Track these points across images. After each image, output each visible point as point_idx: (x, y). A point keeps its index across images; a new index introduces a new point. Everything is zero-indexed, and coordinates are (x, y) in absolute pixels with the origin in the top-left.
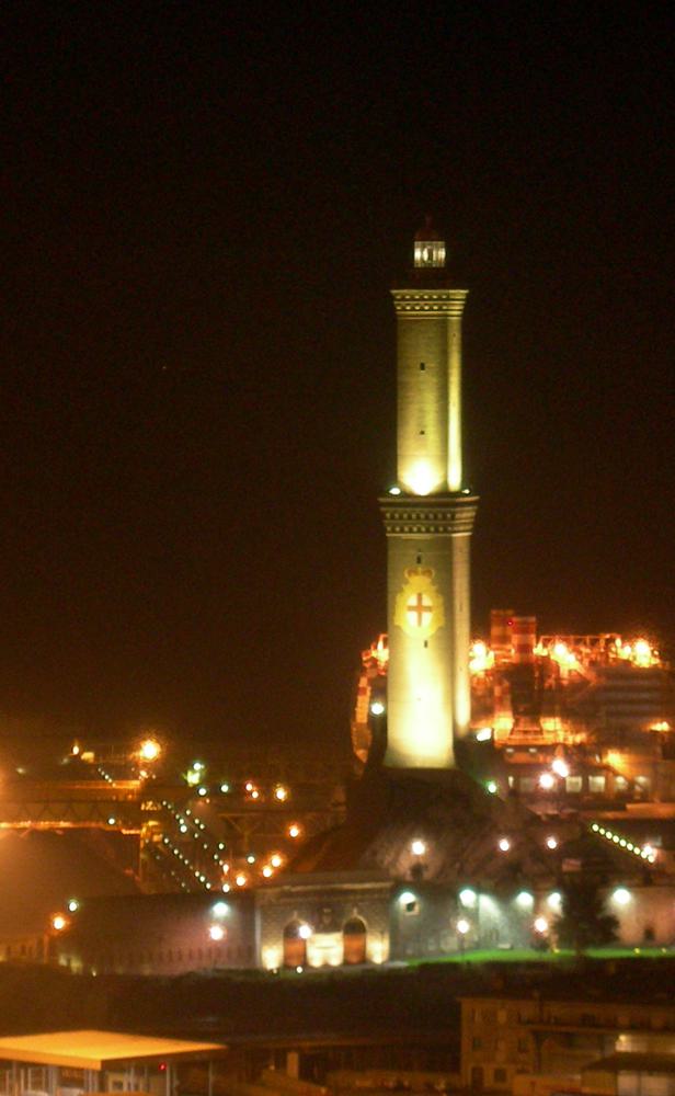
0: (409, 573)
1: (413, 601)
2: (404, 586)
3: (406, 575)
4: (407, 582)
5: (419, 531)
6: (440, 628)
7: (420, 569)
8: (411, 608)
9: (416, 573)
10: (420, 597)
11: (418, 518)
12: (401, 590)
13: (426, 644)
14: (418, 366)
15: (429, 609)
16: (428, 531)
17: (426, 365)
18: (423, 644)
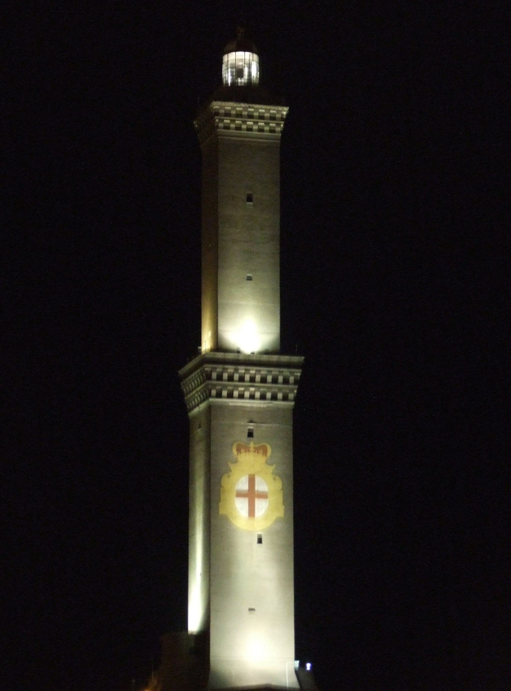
0: (239, 450)
1: (243, 485)
2: (232, 466)
3: (235, 451)
4: (235, 462)
5: (252, 397)
6: (278, 520)
7: (252, 445)
8: (240, 494)
9: (247, 450)
10: (252, 481)
11: (252, 380)
12: (228, 471)
13: (260, 541)
14: (245, 197)
15: (263, 496)
16: (263, 397)
17: (254, 196)
18: (256, 540)
